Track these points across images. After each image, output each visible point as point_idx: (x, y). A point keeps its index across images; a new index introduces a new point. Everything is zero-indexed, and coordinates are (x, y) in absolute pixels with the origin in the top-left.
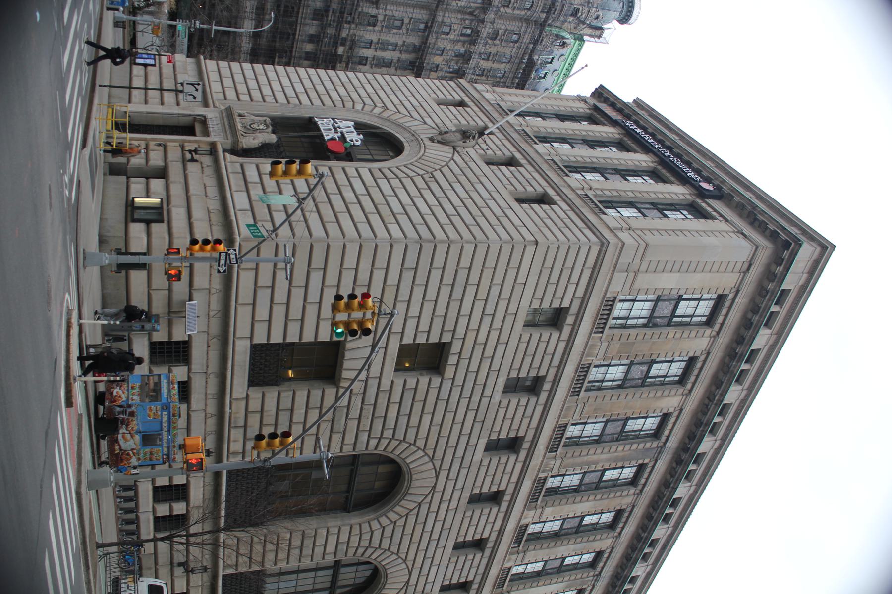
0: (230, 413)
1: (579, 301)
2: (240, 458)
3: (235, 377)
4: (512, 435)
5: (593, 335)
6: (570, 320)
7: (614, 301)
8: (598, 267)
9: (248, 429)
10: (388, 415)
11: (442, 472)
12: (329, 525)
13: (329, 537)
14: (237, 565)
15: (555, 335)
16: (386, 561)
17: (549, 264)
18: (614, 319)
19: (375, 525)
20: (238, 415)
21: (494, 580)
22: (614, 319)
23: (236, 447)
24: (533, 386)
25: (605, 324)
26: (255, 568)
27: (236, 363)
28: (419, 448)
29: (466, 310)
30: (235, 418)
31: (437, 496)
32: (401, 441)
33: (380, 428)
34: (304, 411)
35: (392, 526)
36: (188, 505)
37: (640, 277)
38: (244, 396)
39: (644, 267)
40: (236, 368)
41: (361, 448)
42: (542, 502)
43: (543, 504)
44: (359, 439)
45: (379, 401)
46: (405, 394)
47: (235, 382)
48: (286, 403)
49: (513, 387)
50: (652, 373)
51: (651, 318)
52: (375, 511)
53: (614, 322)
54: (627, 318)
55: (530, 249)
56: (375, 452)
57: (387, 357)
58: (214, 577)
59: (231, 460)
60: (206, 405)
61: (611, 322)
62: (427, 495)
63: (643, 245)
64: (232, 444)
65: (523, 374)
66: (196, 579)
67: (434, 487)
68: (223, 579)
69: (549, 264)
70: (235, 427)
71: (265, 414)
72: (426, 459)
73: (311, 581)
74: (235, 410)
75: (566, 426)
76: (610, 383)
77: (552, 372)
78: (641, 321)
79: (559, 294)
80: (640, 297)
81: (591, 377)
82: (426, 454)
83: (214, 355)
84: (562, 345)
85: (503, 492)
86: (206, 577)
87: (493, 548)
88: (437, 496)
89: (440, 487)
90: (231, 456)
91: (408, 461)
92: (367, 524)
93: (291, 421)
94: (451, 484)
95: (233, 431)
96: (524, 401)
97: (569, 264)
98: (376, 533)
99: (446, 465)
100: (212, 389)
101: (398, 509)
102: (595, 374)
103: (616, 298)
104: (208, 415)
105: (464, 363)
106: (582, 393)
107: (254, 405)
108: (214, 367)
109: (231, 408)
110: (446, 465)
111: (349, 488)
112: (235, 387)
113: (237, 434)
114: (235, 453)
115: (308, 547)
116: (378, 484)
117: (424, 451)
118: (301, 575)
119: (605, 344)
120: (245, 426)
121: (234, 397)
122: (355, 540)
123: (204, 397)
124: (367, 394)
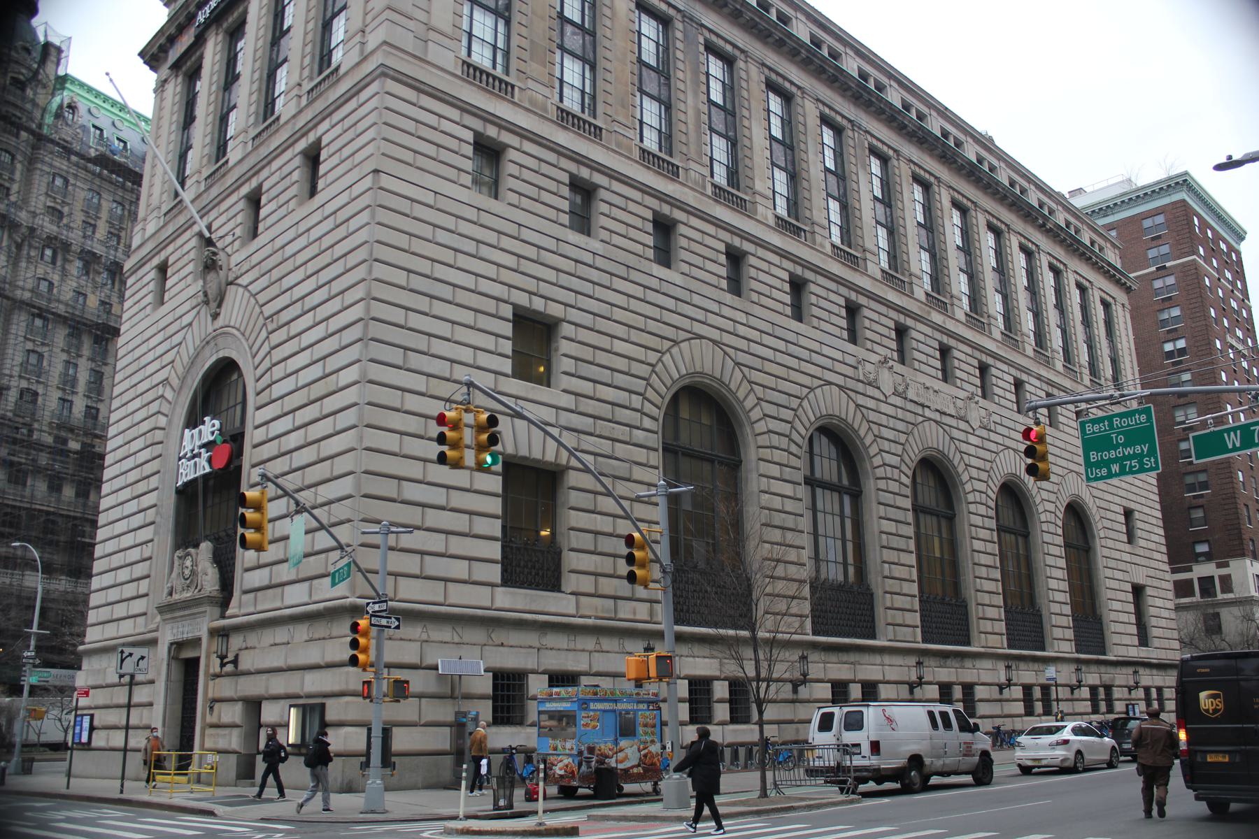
0: (597, 618)
1: (466, 116)
2: (658, 607)
3: (546, 609)
4: (649, 227)
5: (516, 100)
6: (492, 131)
7: (469, 65)
8: (418, 85)
9: (620, 594)
11: (695, 330)
12: (756, 490)
13: (773, 490)
14: (801, 616)
15: (512, 154)
16: (810, 415)
17: (408, 156)
18: (494, 67)
19: (761, 427)
21: (847, 269)
22: (494, 67)
23: (642, 611)
24: (584, 192)
25: (501, 81)
26: (806, 591)
27: (527, 608)
28: (660, 360)
29: (468, 281)
32: (648, 384)
33: (628, 412)
34: (599, 517)
35: (763, 404)
36: (718, 679)
37: (435, 22)
38: (573, 598)
39: (421, 16)
40: (534, 608)
41: (655, 440)
42: (746, 194)
43: (750, 191)
44: (641, 442)
45: (590, 411)
46: (583, 374)
47: (553, 610)
48: (586, 541)
49: (582, 221)
50: (577, 19)
51: (496, 13)
52: (741, 425)
53: (499, 68)
54: (495, 47)
55: (385, 181)
56: (661, 421)
57: (530, 396)
58: (815, 646)
59: (659, 618)
60: (583, 650)
61: (499, 71)
62: (725, 353)
63: (388, 14)
64: (638, 617)
65: (565, 205)
66: (815, 670)
67: (714, 342)
68: (819, 634)
69: (408, 156)
70: (616, 612)
71: (599, 571)
72: (675, 350)
73: (829, 517)
74: (593, 610)
75: (643, 151)
76: (587, 82)
77: (565, 163)
78: (501, 28)
79: (453, 144)
80: (465, 27)
81: (576, 108)
82: (668, 350)
83: (515, 637)
84: (529, 147)
85: (728, 246)
86: (813, 656)
87: (803, 266)
89: (715, 334)
90: (655, 619)
91: (676, 376)
92: (759, 438)
93: (611, 535)
94: (712, 319)
95: (621, 615)
96: (604, 208)
97: (410, 125)
98: (771, 427)
99: (686, 323)
100: (561, 641)
101: (741, 395)
102: (572, 102)
103: (464, 62)
104: (598, 647)
105: (545, 289)
106: (599, 123)
107: (586, 584)
108: (532, 638)
109: (590, 617)
110: (686, 323)
111: (707, 460)
113: (625, 610)
114: (652, 613)
116: (705, 420)
117: (663, 354)
118: (821, 531)
119: (530, 84)
120: (615, 598)
123: (571, 654)
124: (579, 428)
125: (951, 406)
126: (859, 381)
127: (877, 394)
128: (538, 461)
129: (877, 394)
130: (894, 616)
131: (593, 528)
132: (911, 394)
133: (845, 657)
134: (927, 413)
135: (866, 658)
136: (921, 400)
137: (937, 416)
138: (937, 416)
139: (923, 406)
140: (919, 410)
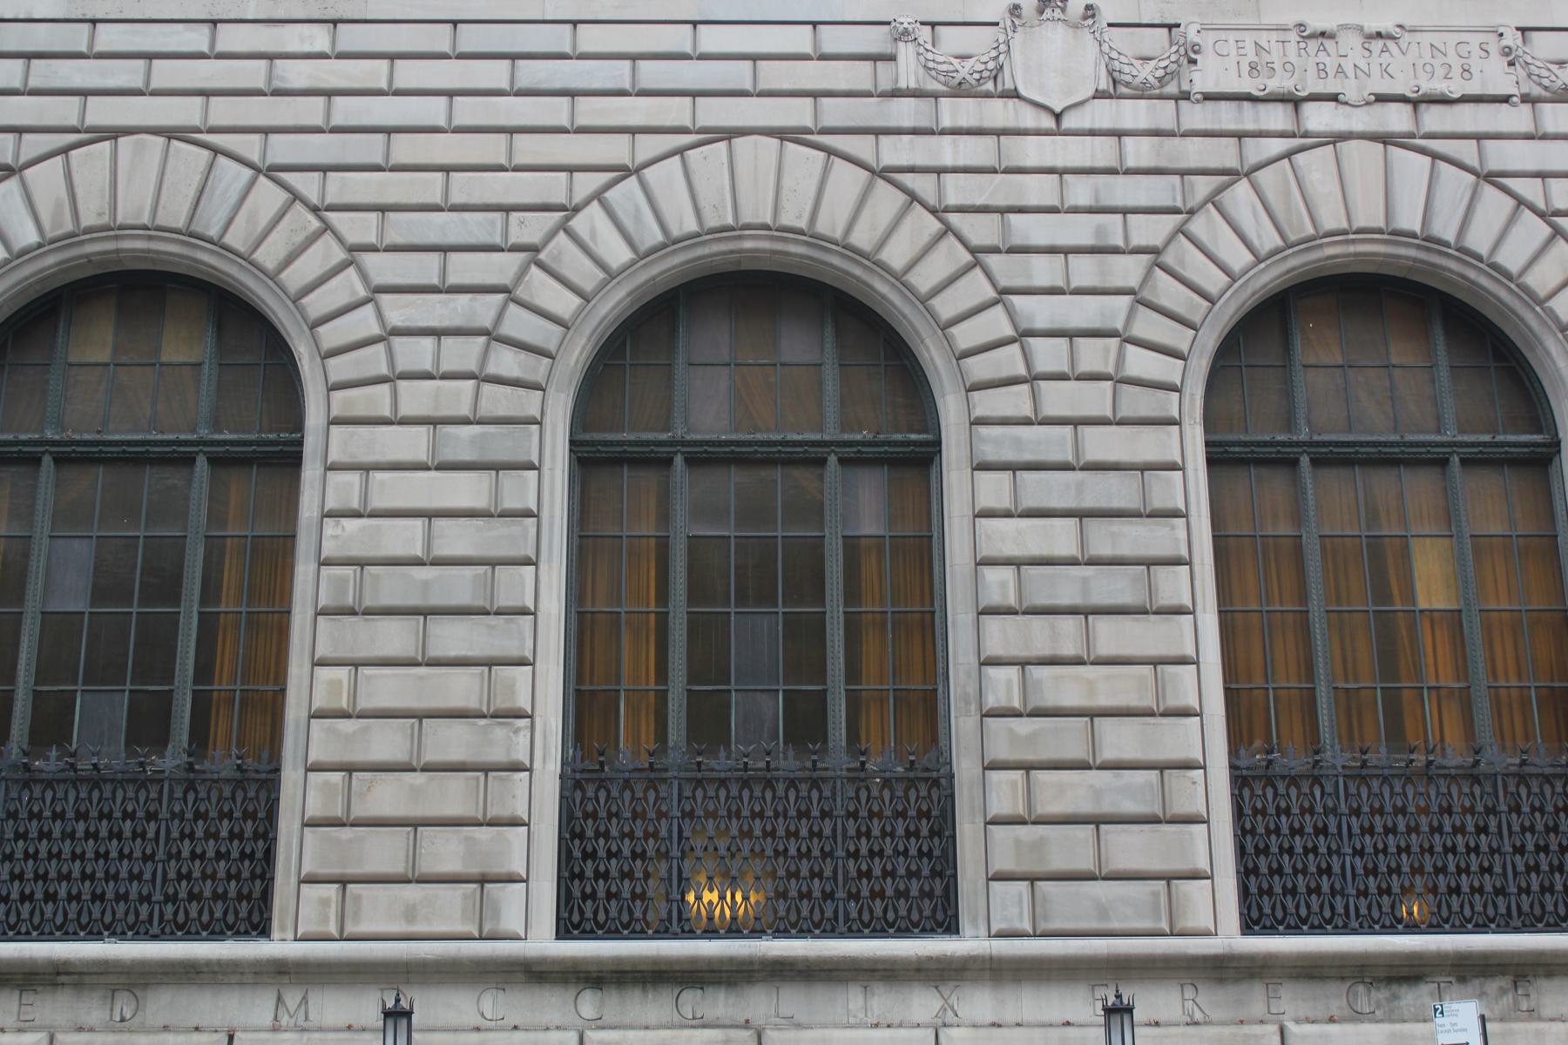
31: (224, 111)
88: (224, 111)
92: (332, 362)
115: (426, 585)
122: (416, 398)
125: (1497, 63)
126: (896, 93)
127: (998, 113)
129: (998, 113)
130: (1039, 846)
132: (1205, 77)
133: (719, 1004)
134: (1319, 118)
135: (853, 999)
136: (1275, 84)
137: (1397, 119)
138: (1397, 119)
139: (1294, 102)
140: (1276, 117)
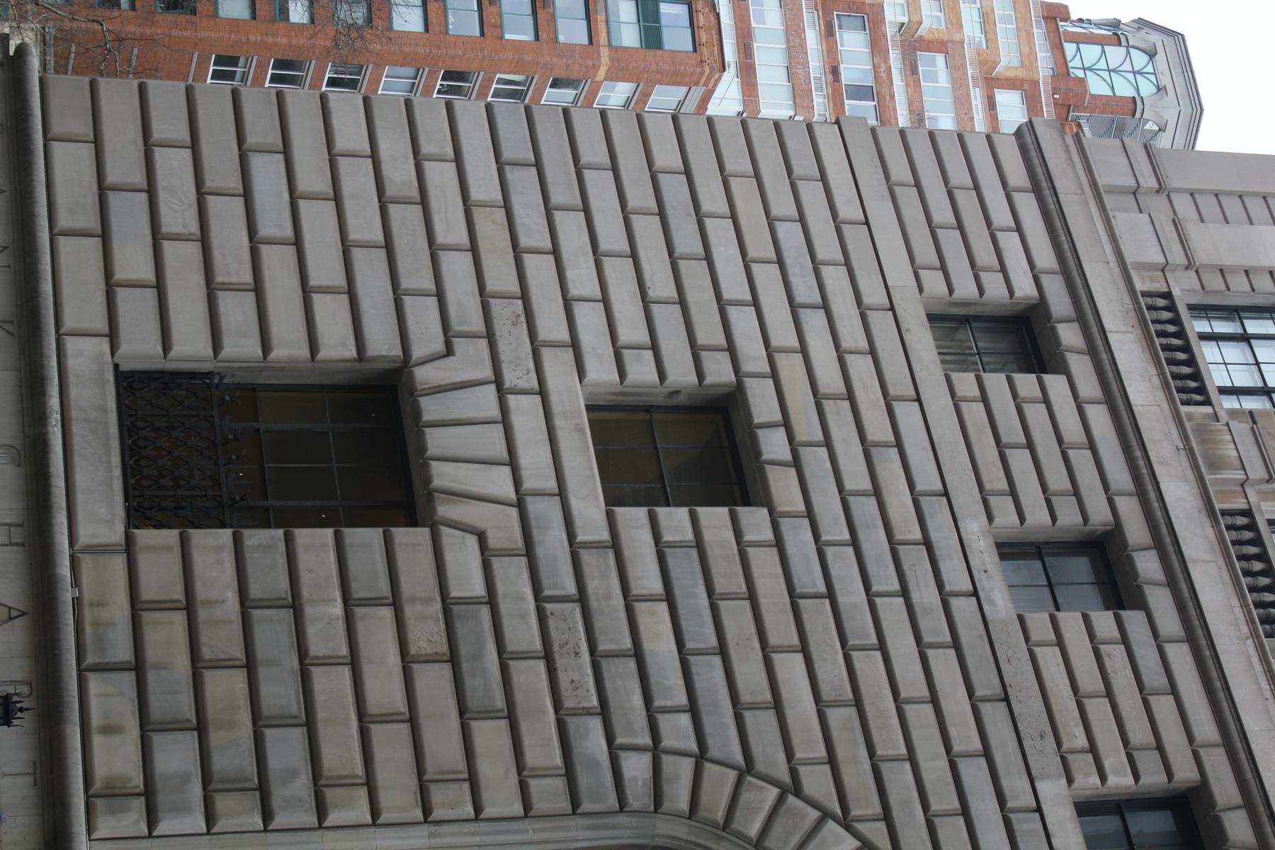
0: (77, 603)
3: (77, 461)
9: (152, 677)
10: (647, 646)
20: (105, 614)
27: (74, 414)
30: (96, 623)
33: (638, 700)
34: (337, 610)
40: (77, 429)
44: (578, 749)
45: (592, 585)
47: (80, 479)
64: (97, 741)
71: (202, 614)
90: (99, 803)
109: (76, 582)
112: (80, 498)
113: (110, 698)
114: (115, 793)
121: (84, 538)
124: (540, 552)
128: (422, 448)
131: (306, 591)
